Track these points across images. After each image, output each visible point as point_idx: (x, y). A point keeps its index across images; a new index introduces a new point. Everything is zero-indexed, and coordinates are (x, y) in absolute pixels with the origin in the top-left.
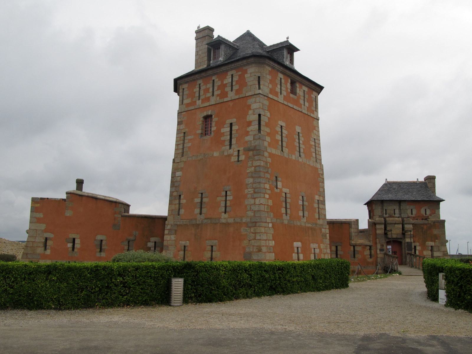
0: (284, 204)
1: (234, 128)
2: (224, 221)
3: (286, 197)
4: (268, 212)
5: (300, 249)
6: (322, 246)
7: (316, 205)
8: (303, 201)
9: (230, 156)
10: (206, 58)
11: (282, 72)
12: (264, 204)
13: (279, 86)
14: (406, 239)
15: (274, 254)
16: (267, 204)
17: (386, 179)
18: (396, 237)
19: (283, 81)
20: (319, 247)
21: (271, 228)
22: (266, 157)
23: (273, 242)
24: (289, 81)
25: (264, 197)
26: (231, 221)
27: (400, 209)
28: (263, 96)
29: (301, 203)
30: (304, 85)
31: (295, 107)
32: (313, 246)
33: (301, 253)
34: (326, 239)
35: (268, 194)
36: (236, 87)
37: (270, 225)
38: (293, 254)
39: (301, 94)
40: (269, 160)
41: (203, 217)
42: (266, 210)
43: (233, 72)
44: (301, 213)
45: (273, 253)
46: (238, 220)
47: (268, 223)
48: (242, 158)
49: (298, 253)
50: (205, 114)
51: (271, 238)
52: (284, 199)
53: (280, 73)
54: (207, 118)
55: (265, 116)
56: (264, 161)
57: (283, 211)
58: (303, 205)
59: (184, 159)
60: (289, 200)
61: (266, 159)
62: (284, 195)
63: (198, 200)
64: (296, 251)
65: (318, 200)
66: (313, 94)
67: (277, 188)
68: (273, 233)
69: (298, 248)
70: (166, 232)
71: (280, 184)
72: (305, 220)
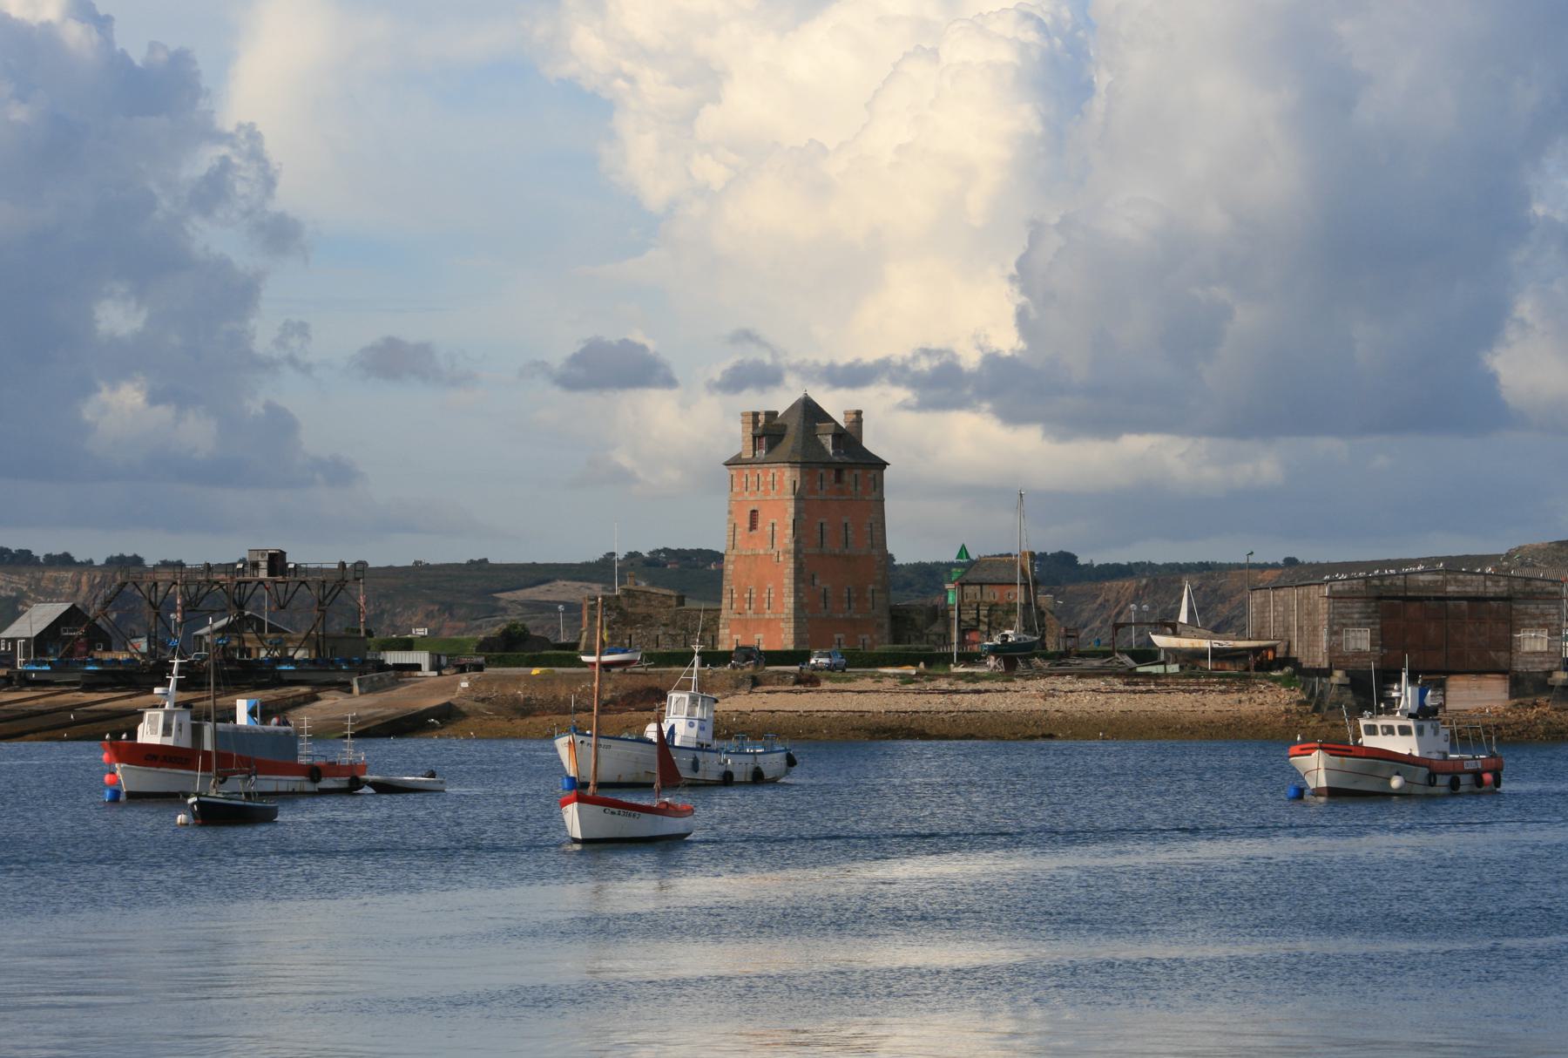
1: (775, 528)
2: (767, 616)
5: (842, 642)
6: (875, 636)
7: (869, 595)
8: (849, 593)
9: (771, 555)
10: (751, 448)
13: (819, 483)
19: (824, 476)
20: (871, 638)
26: (772, 617)
36: (776, 487)
37: (805, 620)
40: (805, 560)
41: (752, 612)
43: (774, 471)
44: (846, 606)
46: (778, 616)
48: (781, 559)
50: (752, 508)
54: (754, 512)
57: (822, 605)
58: (849, 598)
59: (735, 552)
60: (829, 595)
63: (747, 595)
64: (837, 641)
70: (721, 626)
71: (817, 581)
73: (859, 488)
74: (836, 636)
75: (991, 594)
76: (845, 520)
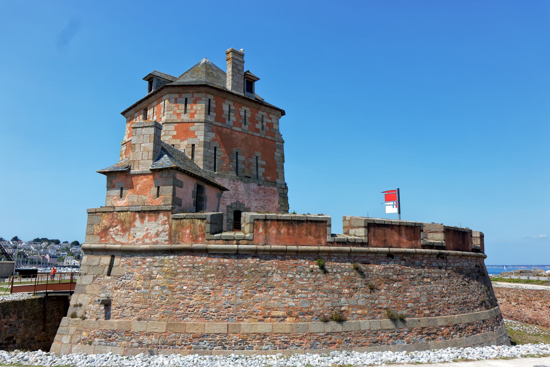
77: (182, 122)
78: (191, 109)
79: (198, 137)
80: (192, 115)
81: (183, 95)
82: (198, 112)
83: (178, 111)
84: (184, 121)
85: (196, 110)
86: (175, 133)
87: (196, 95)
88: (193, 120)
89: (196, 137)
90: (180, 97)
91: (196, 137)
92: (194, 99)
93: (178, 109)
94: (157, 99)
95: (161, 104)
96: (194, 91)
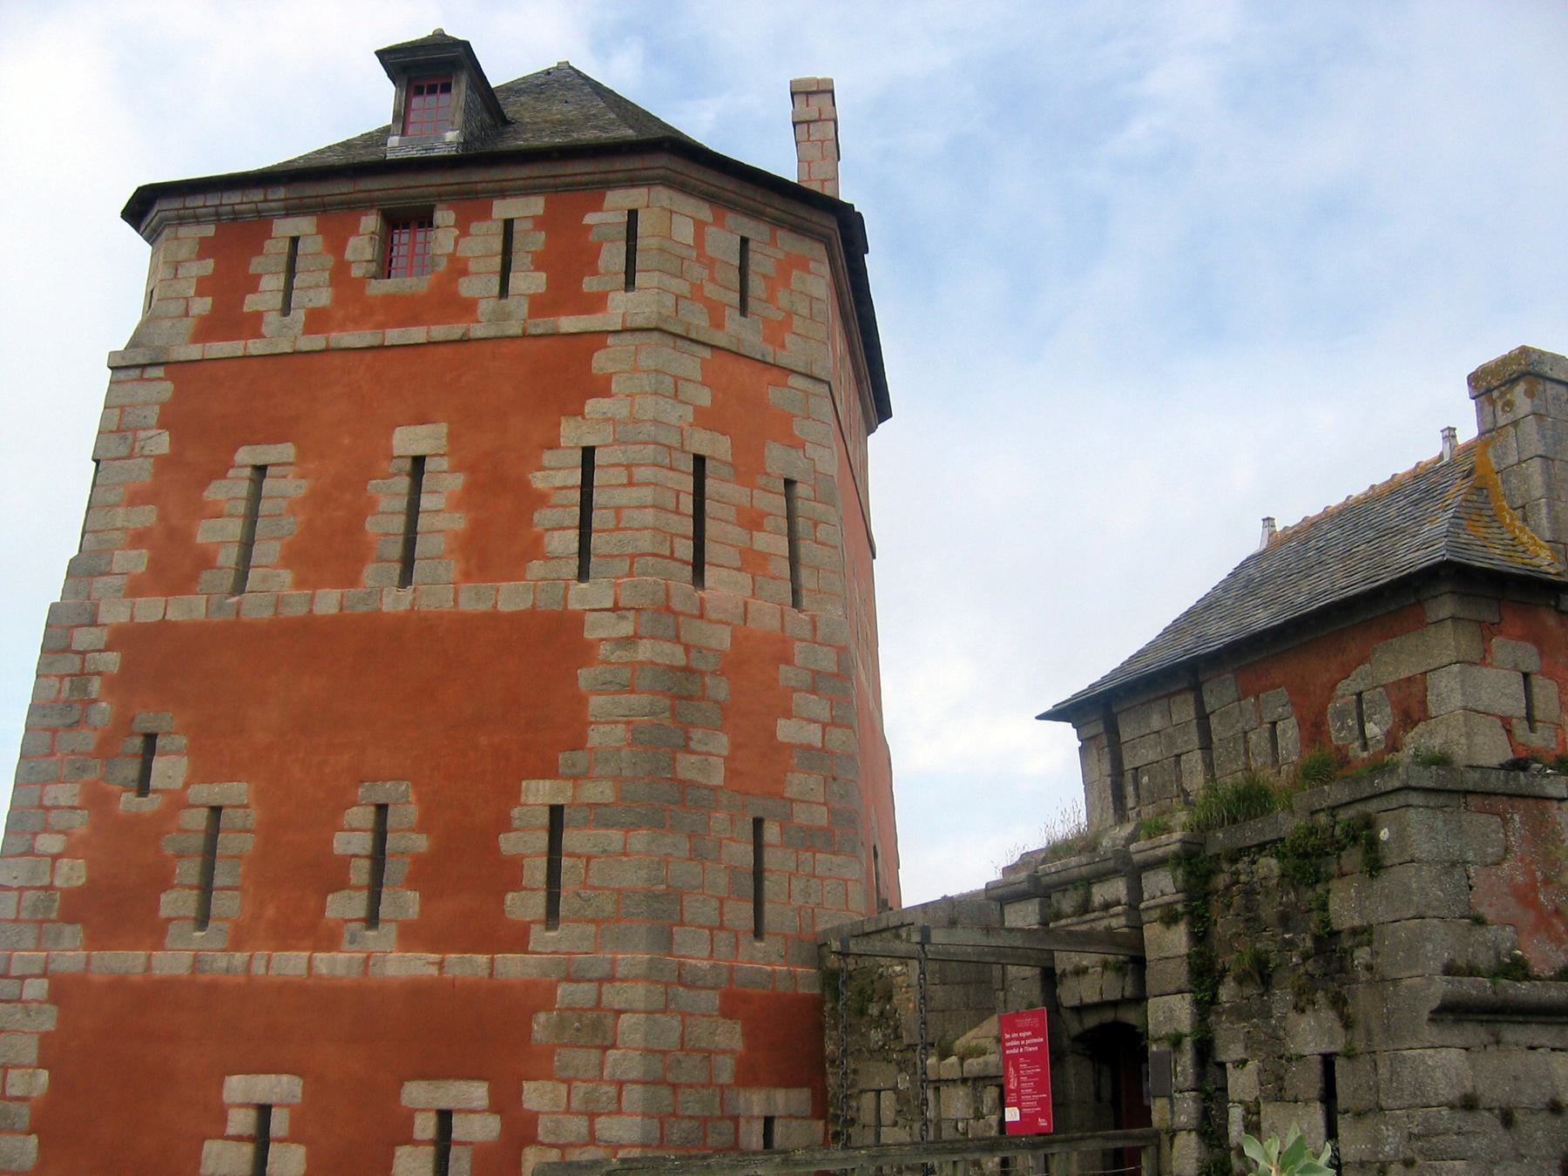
0: (188, 870)
3: (214, 832)
4: (41, 922)
5: (279, 1123)
11: (290, 211)
12: (15, 884)
14: (1152, 1003)
15: (33, 1140)
16: (46, 881)
17: (1268, 521)
18: (1096, 999)
20: (505, 1102)
21: (34, 1005)
22: (83, 653)
23: (44, 1075)
24: (370, 222)
25: (30, 852)
27: (1206, 745)
28: (136, 373)
29: (352, 842)
30: (503, 194)
31: (394, 336)
32: (419, 1095)
33: (293, 1137)
34: (605, 1049)
35: (59, 832)
37: (36, 989)
38: (212, 1147)
39: (483, 242)
42: (24, 915)
45: (29, 1133)
47: (22, 978)
49: (261, 1140)
51: (31, 1054)
52: (198, 841)
53: (287, 215)
55: (130, 457)
56: (62, 678)
61: (84, 662)
62: (196, 819)
64: (241, 1121)
65: (556, 812)
66: (598, 207)
67: (143, 787)
68: (49, 1025)
69: (264, 1111)
71: (169, 770)
72: (386, 935)
73: (529, 281)
74: (237, 1087)
75: (1258, 739)
76: (409, 440)
77: (734, 349)
78: (767, 301)
79: (809, 448)
80: (775, 332)
81: (731, 219)
82: (797, 323)
83: (710, 290)
84: (742, 351)
85: (790, 314)
86: (704, 398)
87: (789, 243)
88: (784, 359)
89: (800, 445)
90: (718, 222)
91: (800, 445)
92: (781, 256)
93: (713, 280)
94: (556, 189)
95: (590, 219)
96: (784, 216)
